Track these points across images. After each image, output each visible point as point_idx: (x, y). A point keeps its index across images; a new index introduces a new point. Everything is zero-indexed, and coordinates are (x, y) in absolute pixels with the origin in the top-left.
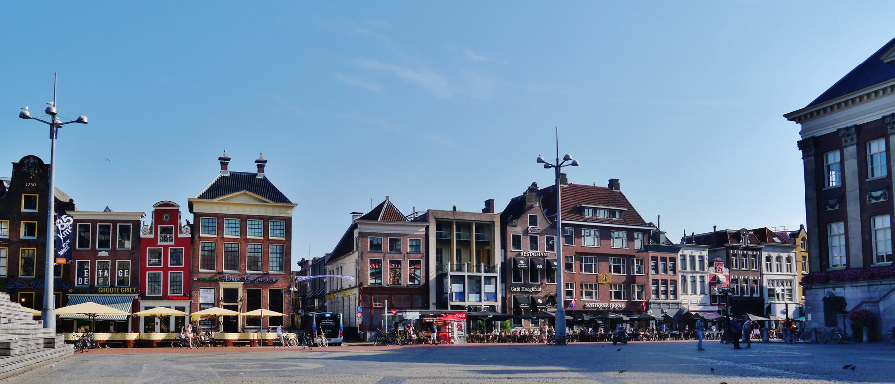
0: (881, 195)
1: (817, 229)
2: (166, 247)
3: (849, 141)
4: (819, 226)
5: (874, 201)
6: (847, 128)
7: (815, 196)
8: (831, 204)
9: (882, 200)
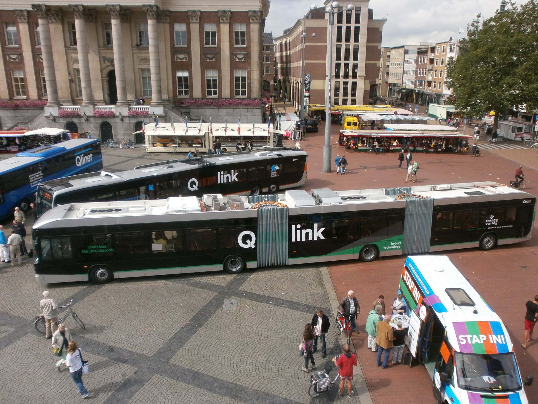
5: (12, 61)
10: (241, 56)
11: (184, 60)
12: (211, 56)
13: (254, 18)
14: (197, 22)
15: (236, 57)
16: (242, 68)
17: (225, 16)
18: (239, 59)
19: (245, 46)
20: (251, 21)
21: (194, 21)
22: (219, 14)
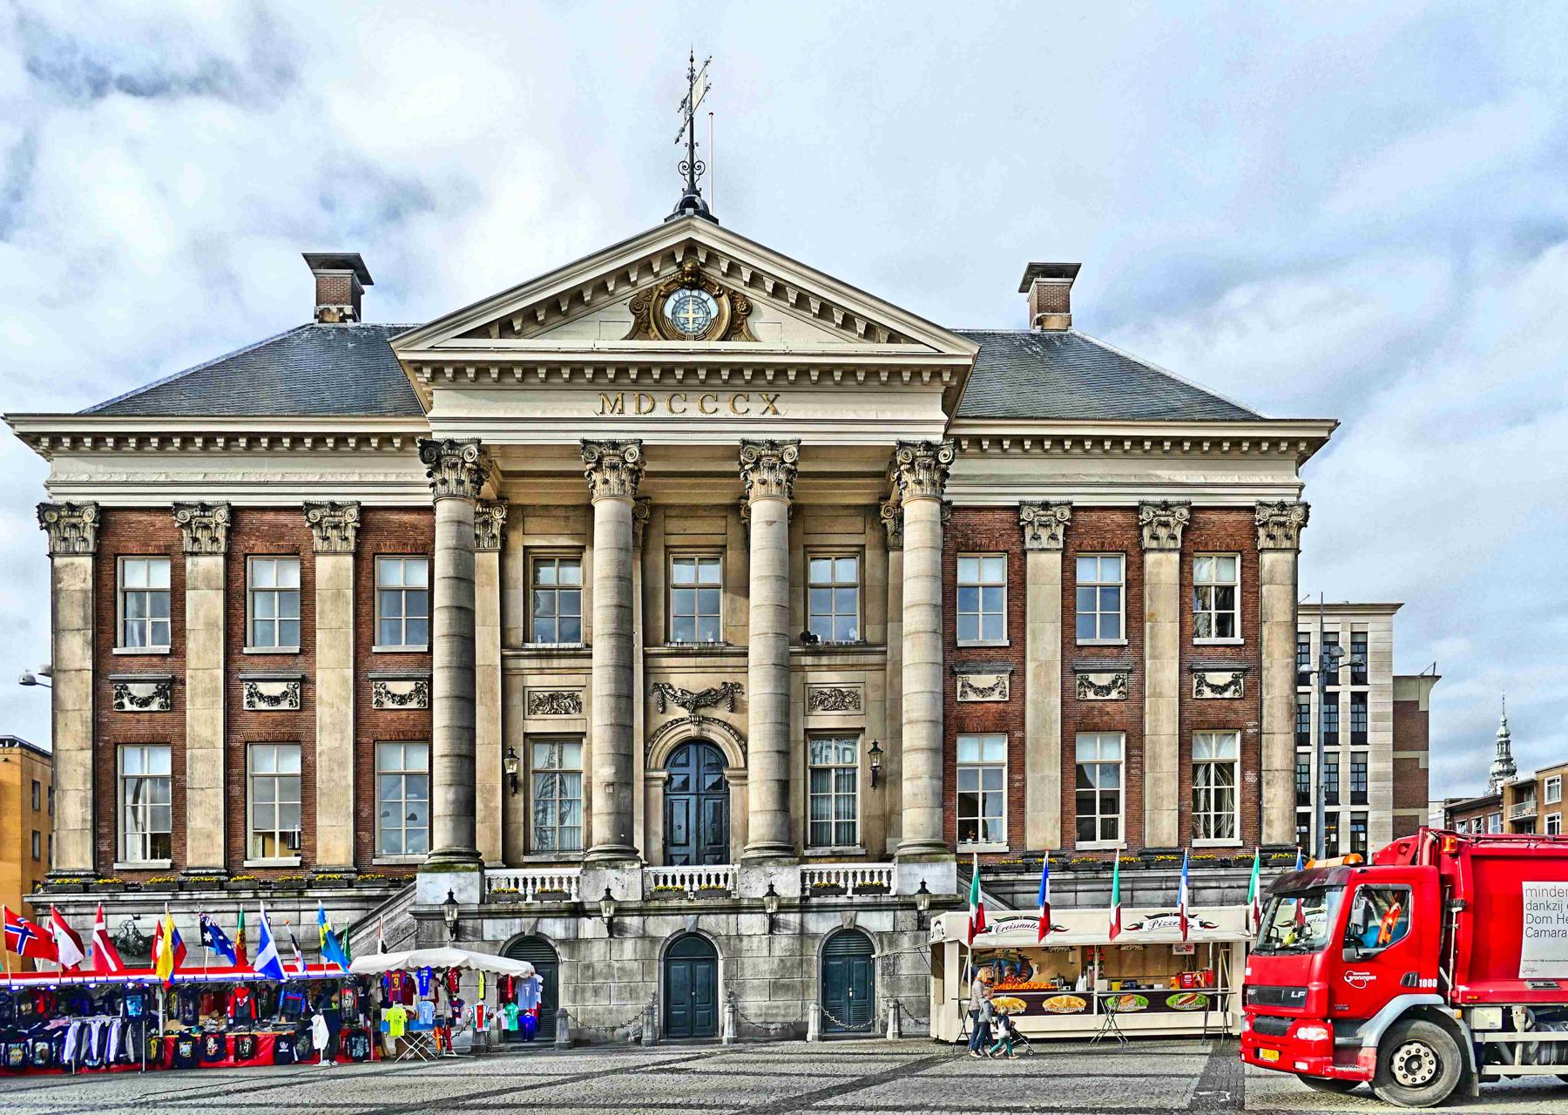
0: (285, 694)
1: (89, 753)
4: (96, 750)
5: (263, 706)
7: (89, 664)
8: (134, 693)
9: (285, 705)
10: (1222, 678)
11: (996, 697)
12: (1104, 680)
13: (1278, 532)
14: (1053, 544)
15: (1202, 681)
16: (1224, 727)
17: (1166, 525)
18: (1214, 688)
19: (1238, 639)
20: (1263, 542)
21: (1045, 542)
22: (1144, 516)
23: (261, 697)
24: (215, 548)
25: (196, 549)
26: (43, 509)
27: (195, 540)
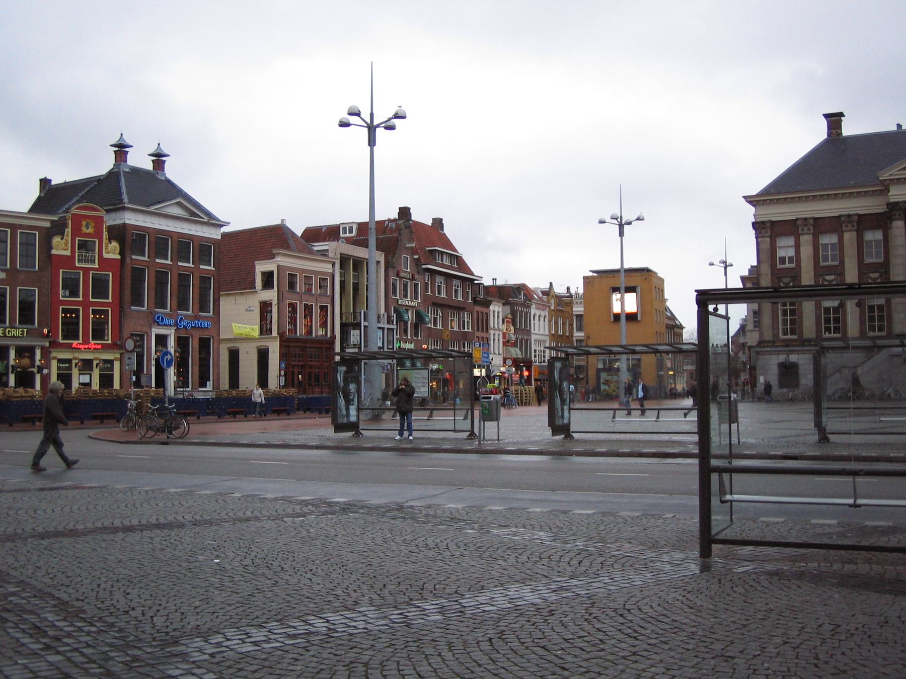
0: (834, 280)
2: (86, 271)
3: (806, 231)
6: (805, 219)
7: (769, 272)
8: (784, 281)
23: (826, 280)
24: (809, 232)
25: (803, 232)
26: (754, 224)
27: (803, 230)
